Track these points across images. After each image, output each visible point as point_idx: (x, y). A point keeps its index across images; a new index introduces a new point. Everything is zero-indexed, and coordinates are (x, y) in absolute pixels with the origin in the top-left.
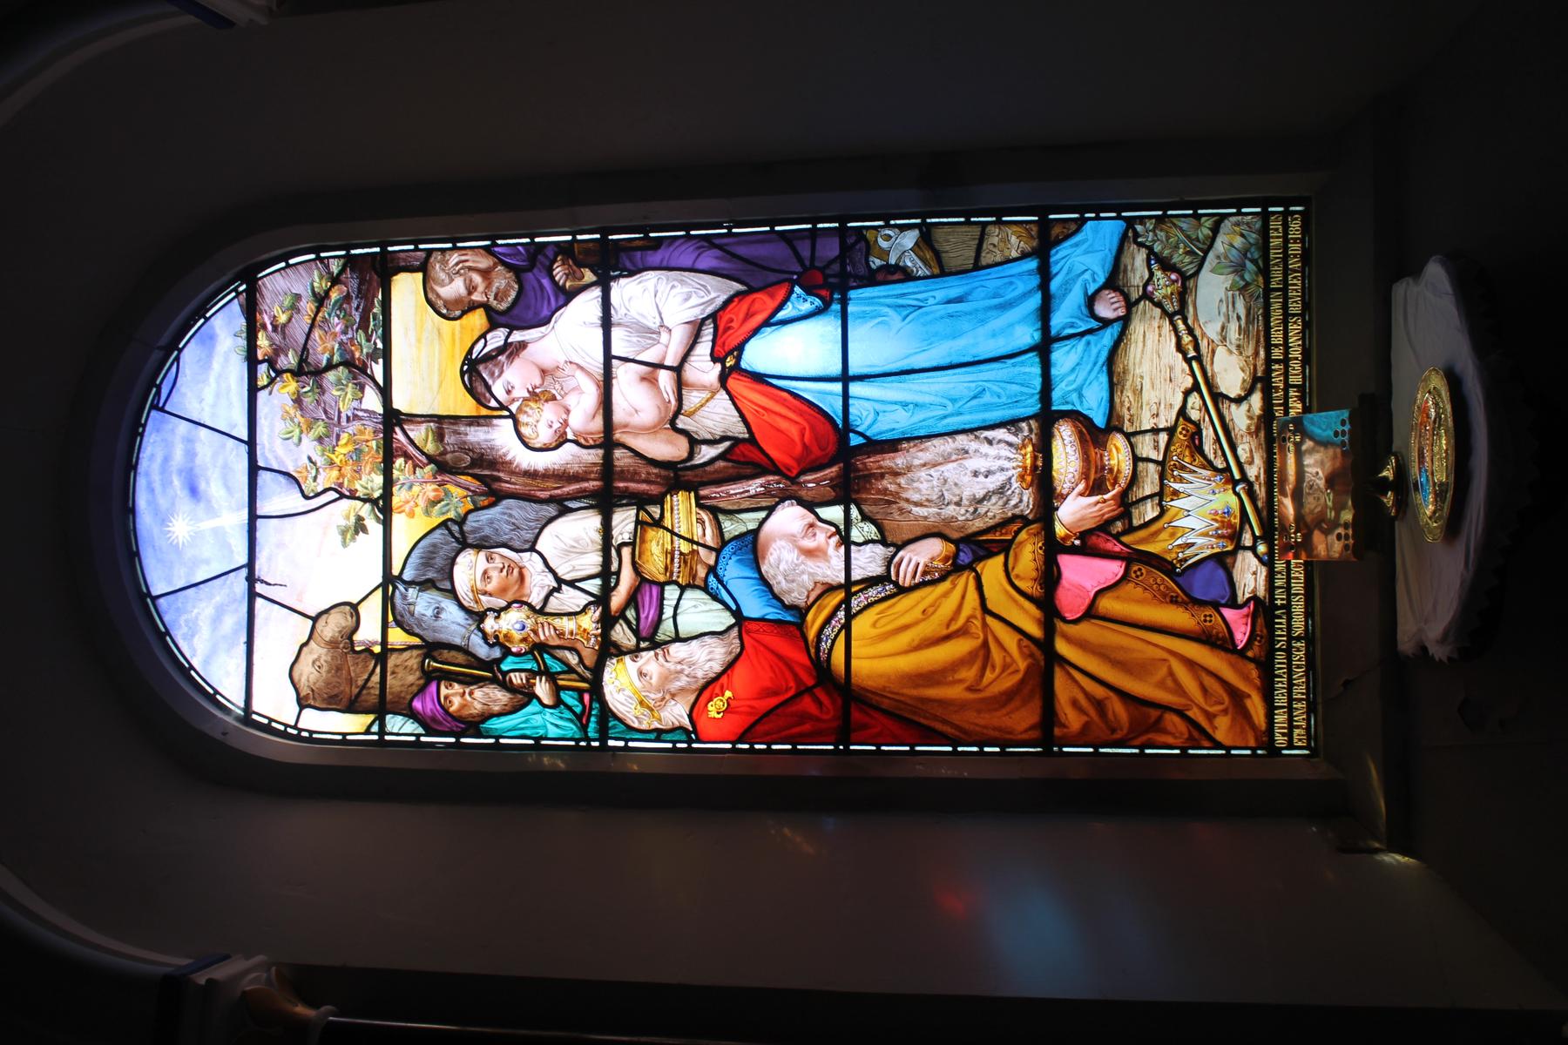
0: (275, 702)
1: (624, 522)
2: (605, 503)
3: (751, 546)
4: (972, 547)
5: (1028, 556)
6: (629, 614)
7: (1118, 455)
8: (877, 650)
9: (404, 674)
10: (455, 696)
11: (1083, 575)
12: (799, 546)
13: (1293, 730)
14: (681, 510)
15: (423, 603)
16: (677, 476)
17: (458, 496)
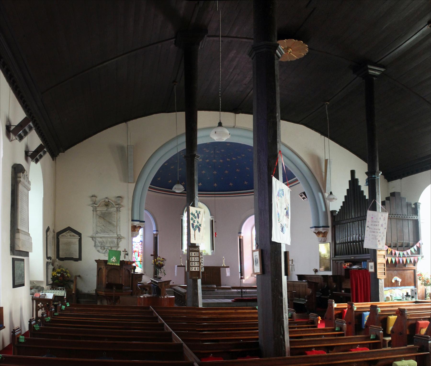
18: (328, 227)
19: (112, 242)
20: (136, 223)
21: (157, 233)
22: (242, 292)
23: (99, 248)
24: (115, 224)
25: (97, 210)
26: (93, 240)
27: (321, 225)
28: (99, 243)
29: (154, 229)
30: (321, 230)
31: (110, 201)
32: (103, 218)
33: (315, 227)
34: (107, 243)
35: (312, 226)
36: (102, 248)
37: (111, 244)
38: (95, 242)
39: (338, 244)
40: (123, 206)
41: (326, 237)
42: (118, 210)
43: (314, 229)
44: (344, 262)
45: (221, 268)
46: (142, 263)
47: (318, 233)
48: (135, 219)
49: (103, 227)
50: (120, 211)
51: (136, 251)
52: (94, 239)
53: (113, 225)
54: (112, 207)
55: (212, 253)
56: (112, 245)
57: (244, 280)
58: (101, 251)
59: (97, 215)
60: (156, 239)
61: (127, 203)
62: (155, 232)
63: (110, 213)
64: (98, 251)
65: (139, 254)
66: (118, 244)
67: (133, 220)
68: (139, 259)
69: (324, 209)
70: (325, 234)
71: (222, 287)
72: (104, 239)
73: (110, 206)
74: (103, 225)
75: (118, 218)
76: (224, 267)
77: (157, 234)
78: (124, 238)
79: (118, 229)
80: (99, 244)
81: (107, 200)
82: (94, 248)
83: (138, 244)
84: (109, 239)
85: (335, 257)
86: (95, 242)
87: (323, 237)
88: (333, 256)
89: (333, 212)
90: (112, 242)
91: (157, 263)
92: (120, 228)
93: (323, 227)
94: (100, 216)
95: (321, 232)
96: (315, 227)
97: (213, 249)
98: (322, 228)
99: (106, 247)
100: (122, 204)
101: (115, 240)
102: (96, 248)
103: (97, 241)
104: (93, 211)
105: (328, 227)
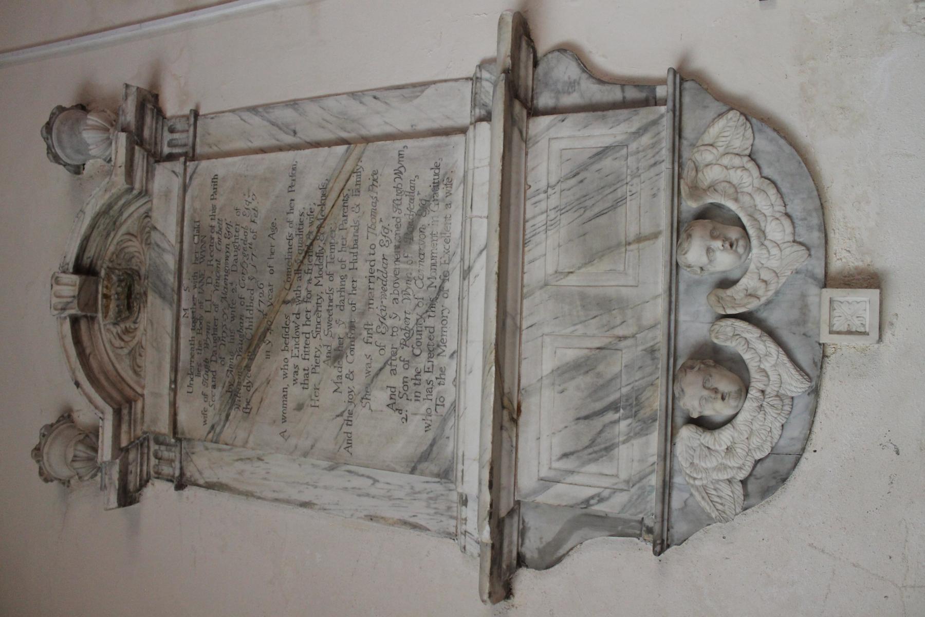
19: (594, 198)
23: (708, 463)
24: (317, 167)
25: (164, 427)
26: (549, 559)
28: (600, 449)
32: (251, 346)
34: (604, 305)
36: (694, 399)
37: (630, 220)
38: (588, 519)
49: (362, 355)
52: (538, 533)
53: (339, 194)
54: (146, 229)
56: (648, 207)
58: (753, 430)
59: (214, 436)
63: (207, 247)
64: (766, 479)
66: (638, 96)
72: (544, 353)
73: (134, 246)
74: (337, 356)
79: (400, 117)
82: (700, 552)
86: (588, 519)
90: (594, 198)
92: (377, 94)
94: (233, 394)
99: (695, 325)
102: (701, 521)
103: (585, 483)
104: (181, 484)
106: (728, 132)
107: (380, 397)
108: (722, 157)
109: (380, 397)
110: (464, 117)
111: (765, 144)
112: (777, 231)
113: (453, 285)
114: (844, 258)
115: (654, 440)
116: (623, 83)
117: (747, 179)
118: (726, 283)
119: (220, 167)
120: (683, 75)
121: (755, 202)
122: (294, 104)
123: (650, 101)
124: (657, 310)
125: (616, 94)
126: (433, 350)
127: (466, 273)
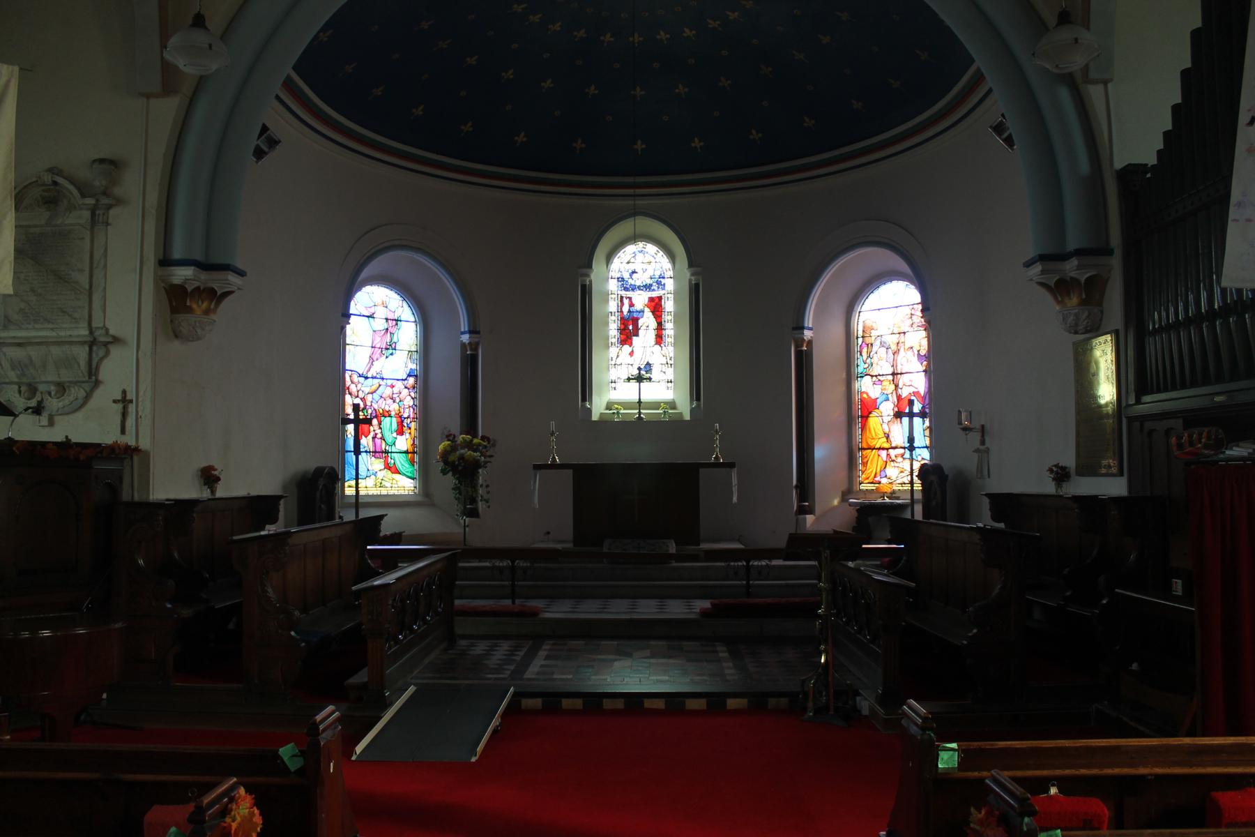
0: (863, 316)
1: (891, 378)
2: (893, 374)
3: (887, 400)
4: (887, 437)
5: (886, 445)
6: (878, 380)
7: (900, 459)
8: (873, 421)
9: (868, 340)
10: (865, 350)
11: (884, 453)
12: (887, 408)
13: (863, 487)
14: (893, 387)
15: (878, 343)
16: (897, 386)
17: (894, 347)
18: (1110, 252)
20: (182, 274)
21: (476, 338)
22: (748, 568)
27: (1071, 245)
29: (464, 326)
30: (1071, 268)
31: (60, 180)
33: (1042, 258)
35: (1031, 253)
39: (1156, 332)
40: (119, 202)
41: (1100, 304)
42: (97, 220)
43: (1037, 268)
44: (1177, 424)
45: (702, 470)
46: (416, 458)
47: (1061, 288)
48: (177, 254)
50: (107, 224)
51: (387, 414)
55: (692, 411)
56: (66, 376)
57: (810, 518)
60: (470, 363)
61: (140, 188)
62: (465, 338)
65: (400, 424)
66: (93, 371)
67: (165, 262)
68: (403, 443)
69: (1085, 167)
70: (1092, 291)
71: (705, 546)
72: (33, 352)
74: (33, 290)
75: (97, 255)
76: (717, 465)
77: (474, 346)
78: (116, 340)
80: (13, 376)
81: (47, 178)
83: (399, 385)
84: (56, 351)
85: (1138, 402)
87: (1084, 303)
88: (1132, 401)
89: (1130, 174)
91: (452, 458)
93: (1079, 253)
95: (1075, 281)
96: (1042, 258)
97: (698, 399)
98: (1074, 262)
99: (41, 387)
100: (117, 191)
101: (82, 353)
105: (1110, 252)
106: (82, 394)
107: (23, 305)
108: (77, 393)
109: (23, 305)
110: (94, 325)
111: (80, 401)
112: (61, 404)
113: (51, 326)
114: (56, 418)
115: (16, 380)
116: (98, 368)
117: (72, 398)
118: (50, 393)
119: (88, 241)
120: (97, 383)
121: (66, 400)
122: (105, 266)
123: (90, 375)
124: (43, 379)
125: (94, 366)
126: (35, 321)
127: (52, 329)
